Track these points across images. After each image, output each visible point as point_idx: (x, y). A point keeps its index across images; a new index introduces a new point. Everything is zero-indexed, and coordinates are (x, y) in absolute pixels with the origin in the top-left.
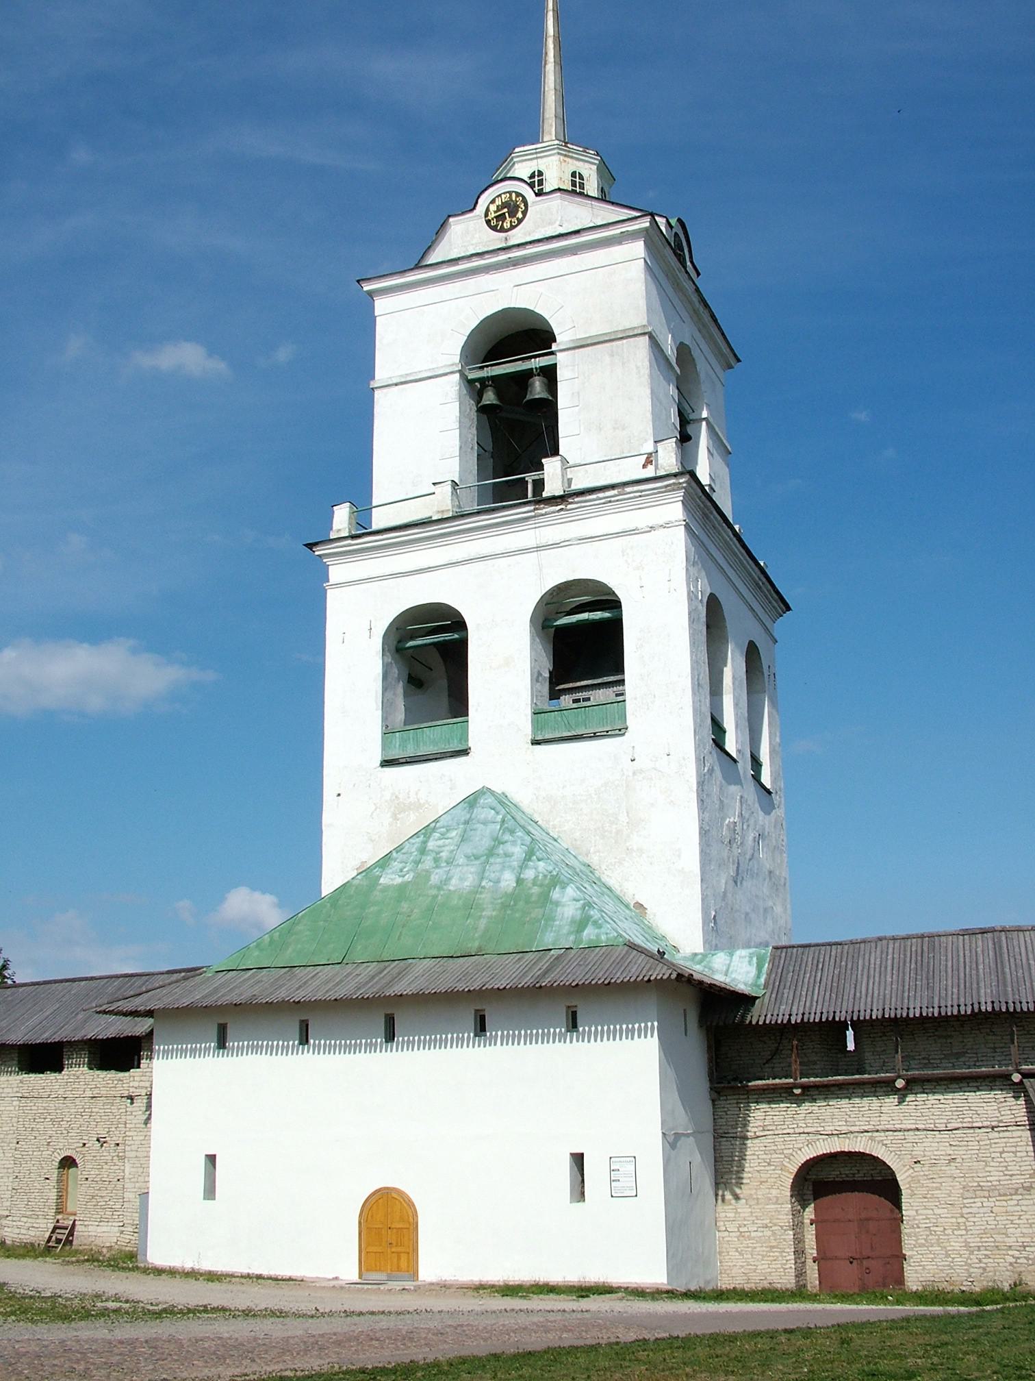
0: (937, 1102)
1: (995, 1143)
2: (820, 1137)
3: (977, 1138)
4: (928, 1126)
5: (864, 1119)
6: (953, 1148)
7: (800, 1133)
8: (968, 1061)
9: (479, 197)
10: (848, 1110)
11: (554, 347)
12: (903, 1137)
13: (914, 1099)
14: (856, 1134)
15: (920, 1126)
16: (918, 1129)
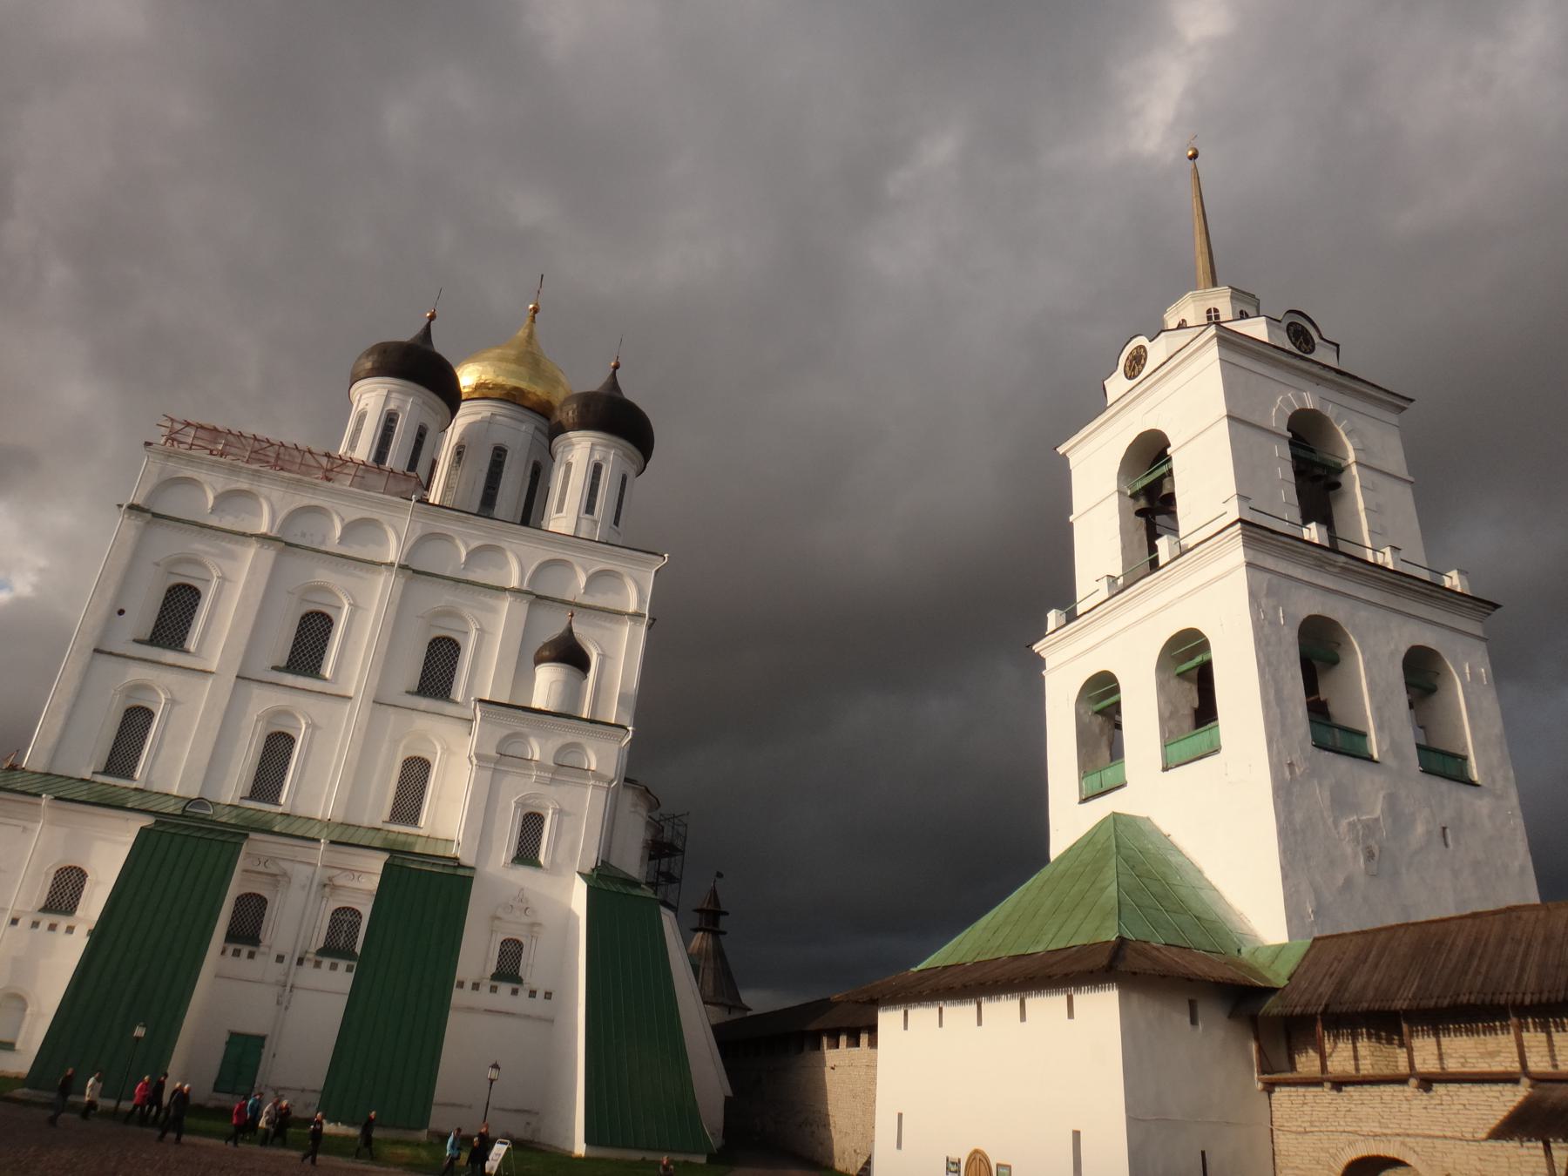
0: (1462, 1107)
1: (1526, 1161)
2: (1358, 1137)
3: (1507, 1154)
4: (1455, 1134)
5: (1395, 1121)
6: (1483, 1163)
7: (1341, 1132)
8: (1504, 1061)
9: (1119, 358)
10: (1380, 1110)
11: (1169, 451)
12: (1432, 1145)
13: (1439, 1102)
14: (1389, 1138)
15: (1448, 1134)
16: (1445, 1137)
